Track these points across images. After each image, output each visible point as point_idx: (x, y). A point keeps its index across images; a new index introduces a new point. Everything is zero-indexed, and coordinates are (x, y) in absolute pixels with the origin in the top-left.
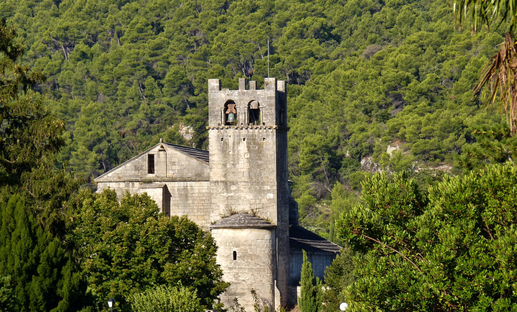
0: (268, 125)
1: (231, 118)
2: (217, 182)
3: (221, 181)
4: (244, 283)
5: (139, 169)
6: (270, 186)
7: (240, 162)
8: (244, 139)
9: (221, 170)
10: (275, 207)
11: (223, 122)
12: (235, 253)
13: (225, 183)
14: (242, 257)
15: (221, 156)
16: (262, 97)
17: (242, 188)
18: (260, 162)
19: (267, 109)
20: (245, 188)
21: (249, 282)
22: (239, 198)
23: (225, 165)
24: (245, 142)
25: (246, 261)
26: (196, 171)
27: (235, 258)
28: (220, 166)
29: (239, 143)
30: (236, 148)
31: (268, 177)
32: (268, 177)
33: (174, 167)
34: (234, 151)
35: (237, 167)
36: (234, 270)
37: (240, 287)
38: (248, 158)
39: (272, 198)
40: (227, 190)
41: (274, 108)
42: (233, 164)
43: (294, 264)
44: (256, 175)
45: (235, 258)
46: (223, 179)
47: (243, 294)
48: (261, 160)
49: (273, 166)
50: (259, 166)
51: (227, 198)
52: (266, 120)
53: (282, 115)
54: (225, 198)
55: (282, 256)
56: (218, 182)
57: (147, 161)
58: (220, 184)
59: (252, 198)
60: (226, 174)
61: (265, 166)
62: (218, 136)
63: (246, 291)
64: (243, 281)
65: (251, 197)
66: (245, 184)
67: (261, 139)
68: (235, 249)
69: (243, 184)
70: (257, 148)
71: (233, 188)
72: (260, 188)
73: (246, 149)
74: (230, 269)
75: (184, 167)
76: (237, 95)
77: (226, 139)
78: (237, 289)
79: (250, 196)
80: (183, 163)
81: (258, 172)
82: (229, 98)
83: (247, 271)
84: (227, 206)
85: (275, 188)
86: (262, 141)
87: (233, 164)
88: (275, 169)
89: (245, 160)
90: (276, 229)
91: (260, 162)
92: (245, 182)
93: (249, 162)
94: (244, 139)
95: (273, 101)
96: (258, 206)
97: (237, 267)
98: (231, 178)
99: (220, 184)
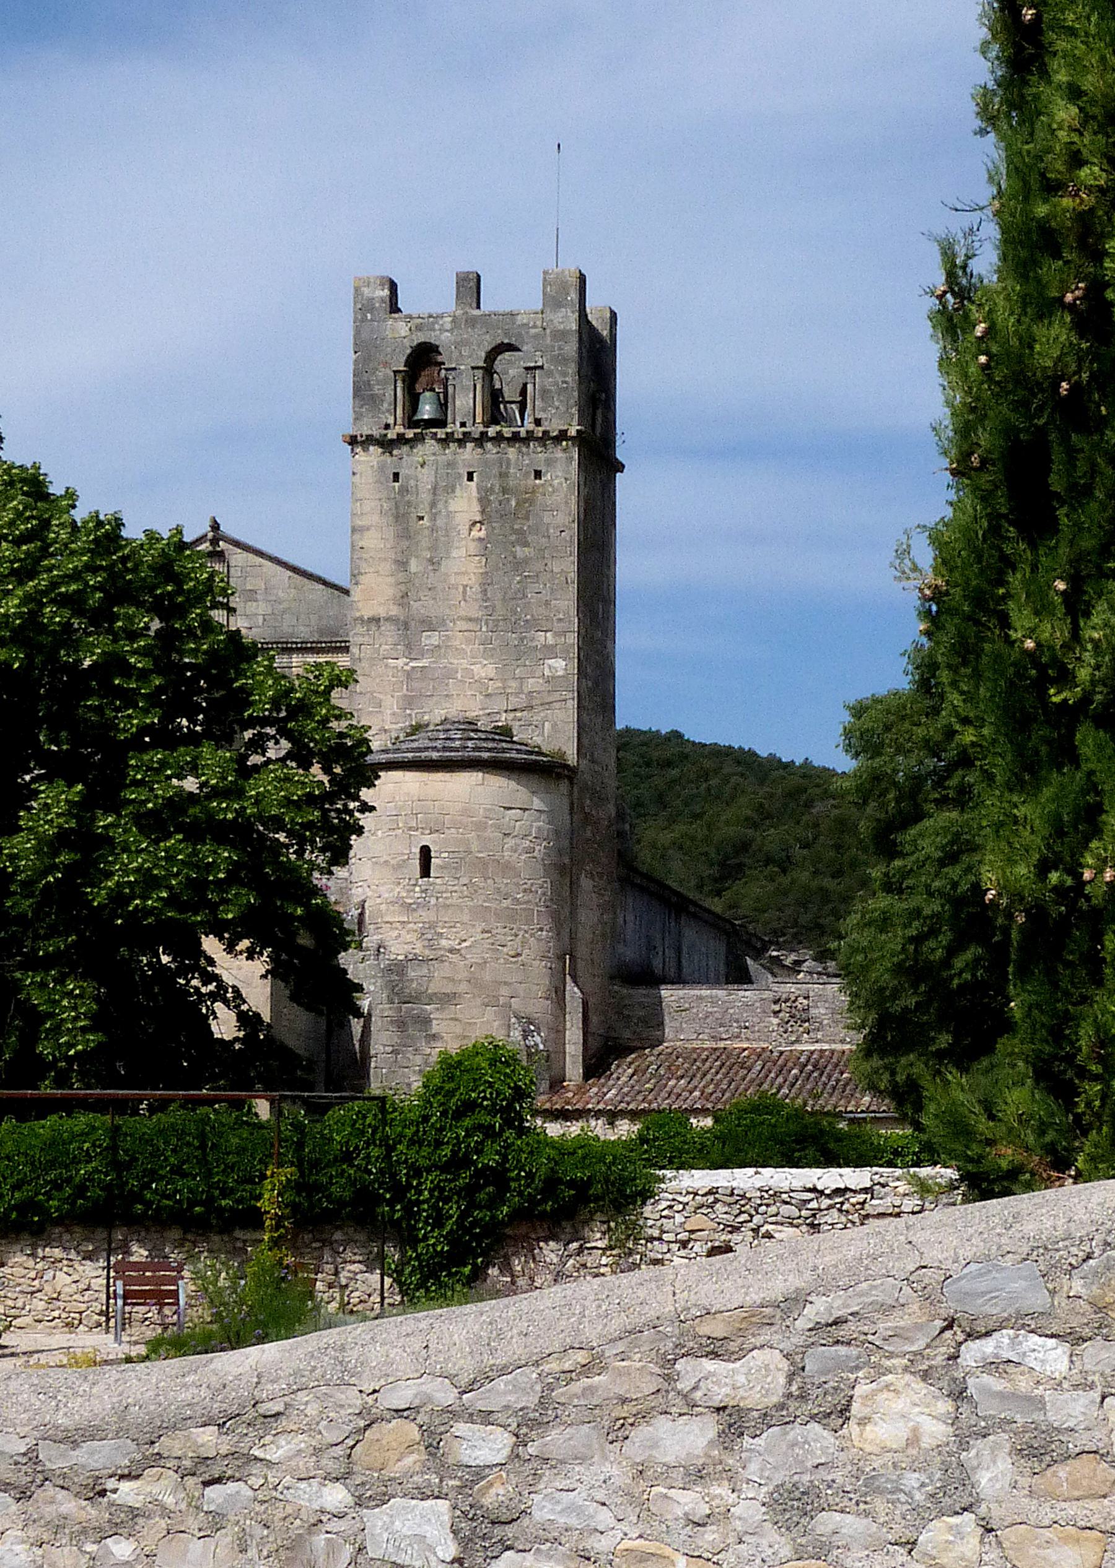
0: (554, 426)
1: (427, 411)
2: (375, 620)
3: (387, 619)
4: (454, 958)
6: (557, 634)
7: (455, 553)
8: (470, 477)
9: (391, 580)
10: (572, 704)
11: (399, 421)
12: (425, 854)
14: (453, 868)
15: (390, 533)
16: (533, 331)
17: (458, 640)
19: (550, 374)
20: (468, 641)
21: (472, 958)
22: (450, 674)
23: (402, 564)
24: (473, 484)
25: (464, 880)
26: (320, 618)
27: (425, 872)
28: (387, 567)
29: (451, 489)
30: (440, 505)
33: (251, 607)
34: (434, 518)
35: (443, 569)
36: (425, 915)
37: (440, 972)
38: (480, 539)
39: (561, 673)
40: (409, 646)
41: (572, 369)
42: (431, 561)
43: (630, 918)
44: (510, 595)
45: (425, 872)
46: (394, 611)
47: (448, 999)
48: (526, 544)
49: (567, 566)
50: (518, 565)
52: (544, 410)
53: (599, 412)
54: (402, 677)
55: (592, 878)
58: (386, 627)
61: (538, 566)
62: (382, 468)
63: (463, 987)
64: (451, 951)
65: (490, 670)
66: (471, 626)
67: (527, 473)
68: (426, 840)
69: (462, 626)
70: (513, 503)
71: (431, 639)
72: (522, 639)
73: (476, 507)
74: (408, 908)
75: (285, 605)
76: (448, 326)
77: (408, 477)
78: (430, 978)
79: (484, 669)
81: (515, 586)
82: (420, 338)
83: (466, 918)
84: (409, 702)
85: (572, 639)
86: (531, 481)
87: (431, 561)
88: (573, 576)
89: (473, 547)
90: (571, 780)
91: (520, 552)
92: (470, 620)
93: (485, 553)
94: (470, 477)
95: (571, 348)
96: (514, 702)
97: (433, 901)
98: (421, 607)
99: (386, 627)
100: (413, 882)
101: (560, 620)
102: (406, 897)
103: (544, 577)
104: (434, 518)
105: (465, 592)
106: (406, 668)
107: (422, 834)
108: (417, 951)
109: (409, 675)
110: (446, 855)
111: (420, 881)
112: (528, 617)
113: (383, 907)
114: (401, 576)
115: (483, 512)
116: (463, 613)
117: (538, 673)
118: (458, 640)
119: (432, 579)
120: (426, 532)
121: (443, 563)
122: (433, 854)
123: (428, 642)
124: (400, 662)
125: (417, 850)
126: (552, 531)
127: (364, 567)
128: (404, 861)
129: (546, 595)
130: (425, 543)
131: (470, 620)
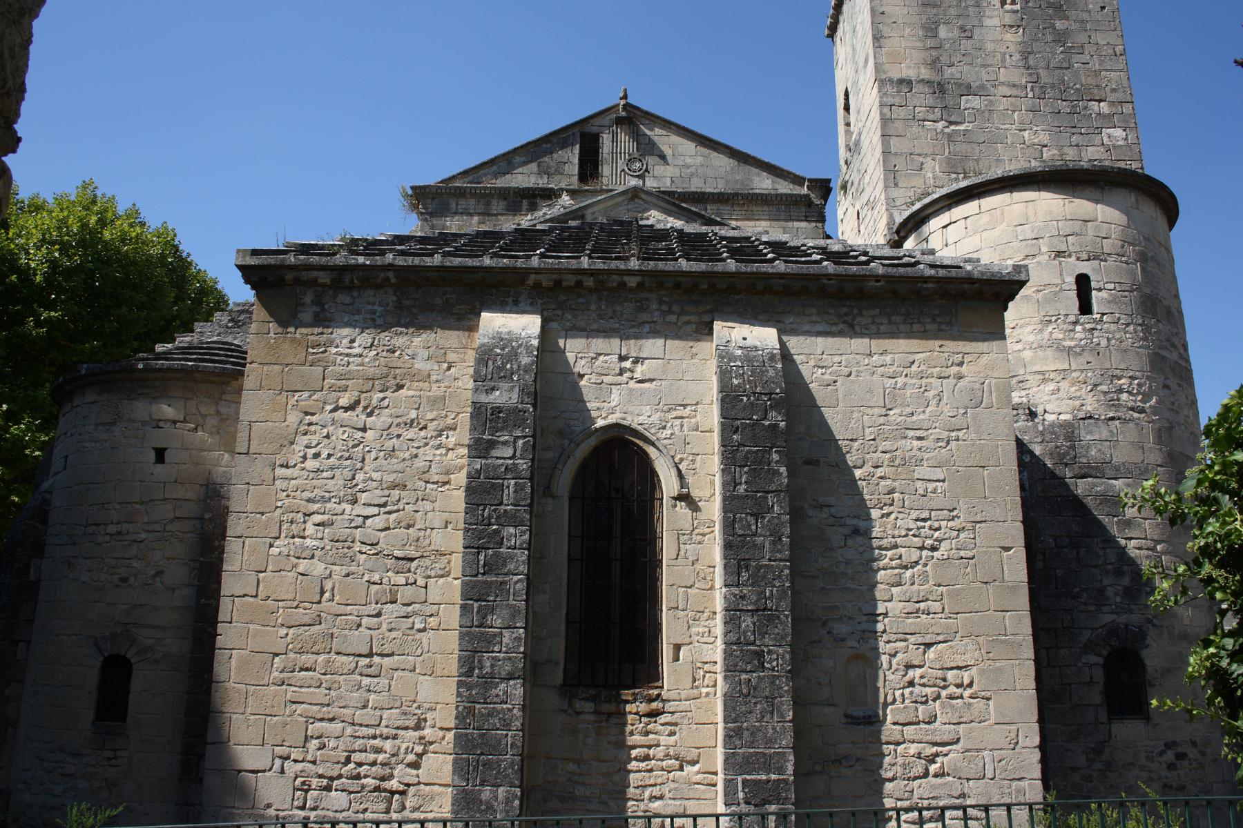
6: (1112, 104)
7: (987, 22)
9: (920, 44)
12: (1083, 283)
13: (939, 88)
17: (1003, 104)
23: (931, 30)
26: (727, 182)
31: (1096, 74)
32: (1096, 74)
39: (1120, 143)
42: (963, 29)
46: (925, 73)
48: (1067, 18)
51: (949, 135)
56: (909, 82)
66: (1014, 92)
68: (1085, 268)
75: (693, 169)
80: (688, 160)
91: (1060, 25)
92: (1014, 86)
100: (1072, 318)
101: (1113, 90)
102: (1064, 339)
103: (1088, 49)
105: (1003, 61)
106: (946, 130)
107: (1078, 259)
108: (1089, 408)
109: (950, 138)
110: (1111, 286)
111: (1083, 318)
112: (1077, 86)
113: (1027, 354)
114: (930, 43)
116: (1002, 79)
117: (1097, 141)
118: (1003, 104)
121: (977, 32)
122: (1093, 284)
123: (968, 106)
124: (940, 125)
125: (1070, 279)
126: (1091, 6)
127: (886, 31)
128: (1056, 294)
129: (1095, 64)
131: (1014, 86)
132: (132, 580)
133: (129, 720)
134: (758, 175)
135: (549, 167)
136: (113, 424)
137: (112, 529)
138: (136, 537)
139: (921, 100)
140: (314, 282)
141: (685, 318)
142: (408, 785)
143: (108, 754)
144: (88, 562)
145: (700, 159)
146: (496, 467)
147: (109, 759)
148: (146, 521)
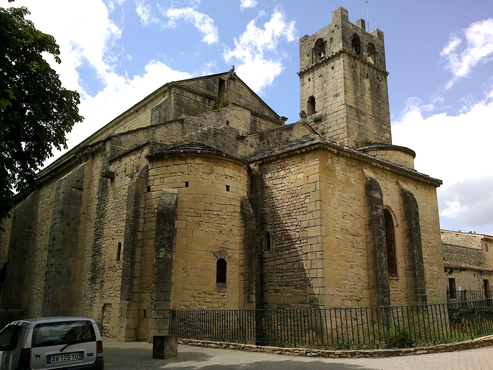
5: (211, 89)
7: (366, 95)
13: (357, 111)
17: (369, 120)
18: (379, 101)
23: (355, 93)
28: (352, 92)
30: (362, 80)
31: (385, 117)
32: (385, 117)
34: (361, 82)
42: (361, 94)
46: (355, 106)
48: (380, 99)
57: (218, 85)
58: (353, 110)
59: (376, 133)
60: (356, 102)
69: (369, 116)
91: (379, 101)
92: (371, 115)
101: (387, 123)
104: (361, 82)
115: (371, 86)
119: (362, 100)
120: (360, 86)
129: (384, 115)
130: (360, 89)
132: (223, 231)
133: (227, 282)
134: (266, 110)
135: (210, 88)
136: (210, 174)
137: (215, 213)
138: (223, 217)
139: (354, 113)
140: (333, 152)
141: (394, 180)
142: (360, 298)
143: (222, 294)
144: (207, 224)
145: (251, 100)
146: (379, 214)
147: (223, 296)
148: (225, 211)
